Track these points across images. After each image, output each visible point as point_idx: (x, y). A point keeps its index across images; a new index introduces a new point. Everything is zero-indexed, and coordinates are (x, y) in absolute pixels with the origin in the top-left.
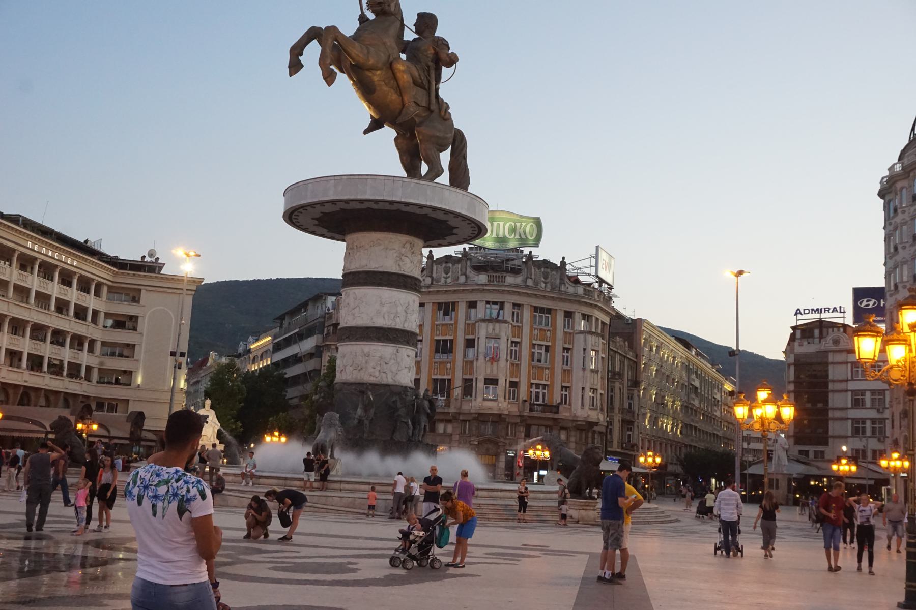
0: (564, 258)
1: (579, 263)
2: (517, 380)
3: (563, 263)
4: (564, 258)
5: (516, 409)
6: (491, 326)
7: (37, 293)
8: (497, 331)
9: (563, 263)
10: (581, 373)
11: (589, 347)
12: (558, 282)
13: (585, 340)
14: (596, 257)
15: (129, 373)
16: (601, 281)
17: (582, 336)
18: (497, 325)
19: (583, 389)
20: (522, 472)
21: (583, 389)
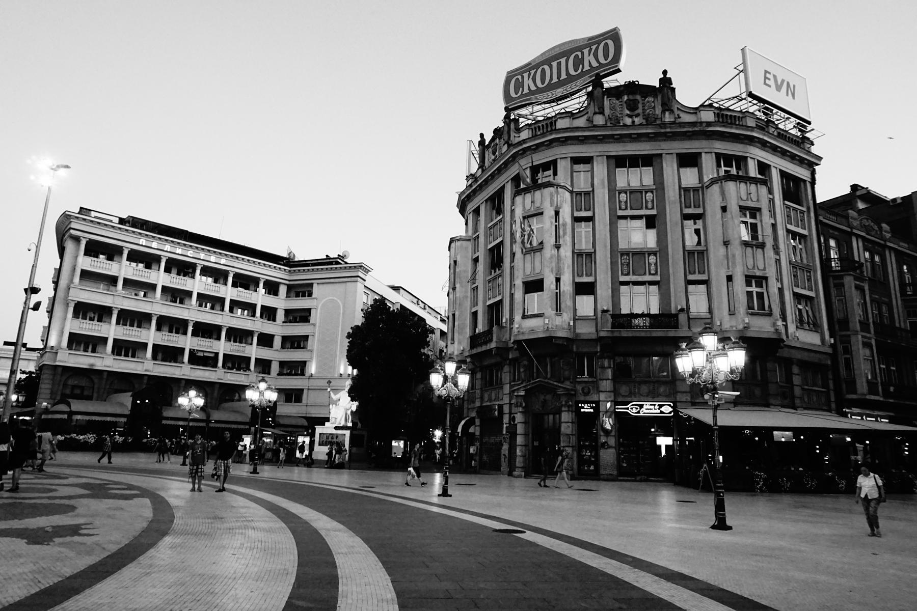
0: (665, 72)
1: (729, 94)
2: (590, 279)
3: (666, 81)
4: (665, 72)
5: (593, 330)
6: (528, 197)
7: (163, 287)
8: (538, 204)
9: (666, 81)
10: (722, 250)
11: (733, 207)
12: (658, 111)
13: (723, 193)
14: (744, 63)
15: (303, 364)
16: (768, 106)
17: (716, 188)
18: (538, 194)
19: (730, 278)
20: (612, 441)
21: (730, 278)
